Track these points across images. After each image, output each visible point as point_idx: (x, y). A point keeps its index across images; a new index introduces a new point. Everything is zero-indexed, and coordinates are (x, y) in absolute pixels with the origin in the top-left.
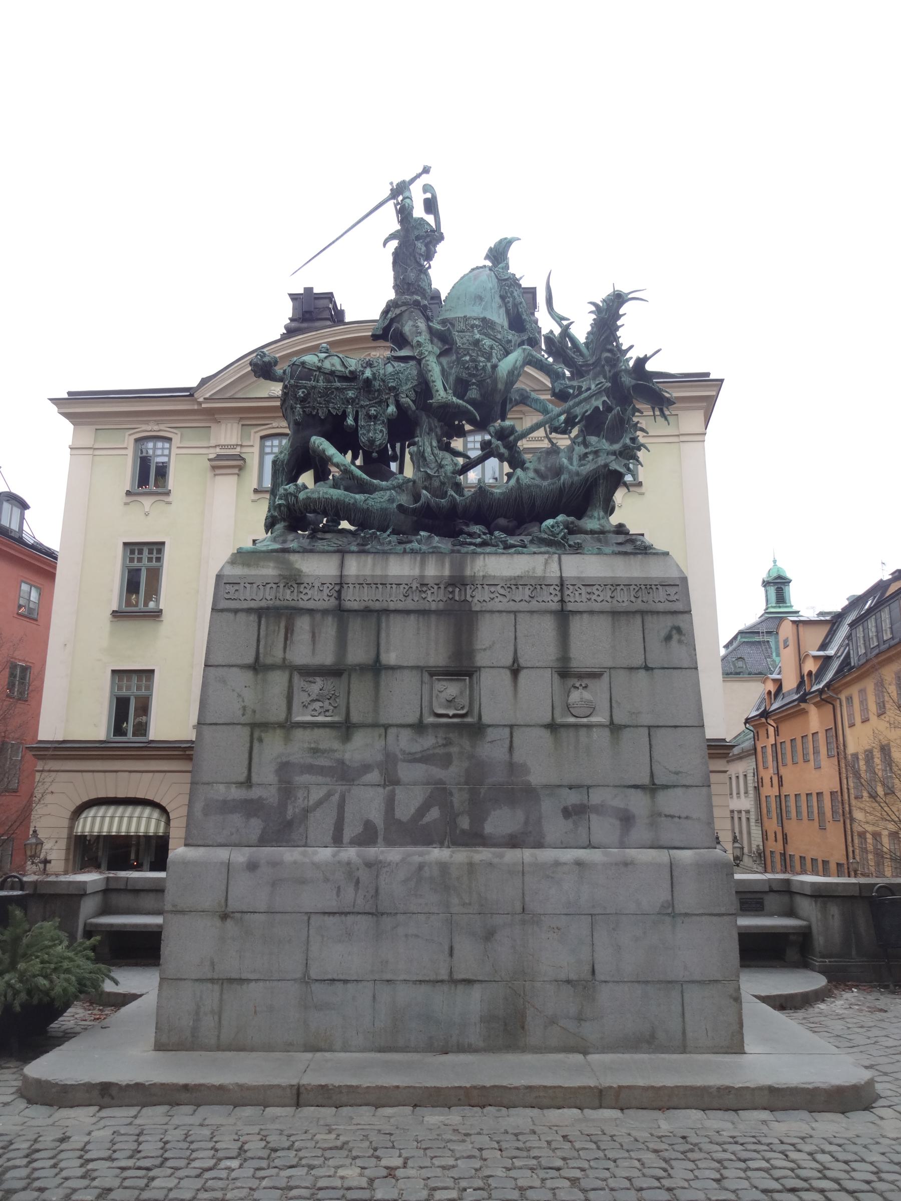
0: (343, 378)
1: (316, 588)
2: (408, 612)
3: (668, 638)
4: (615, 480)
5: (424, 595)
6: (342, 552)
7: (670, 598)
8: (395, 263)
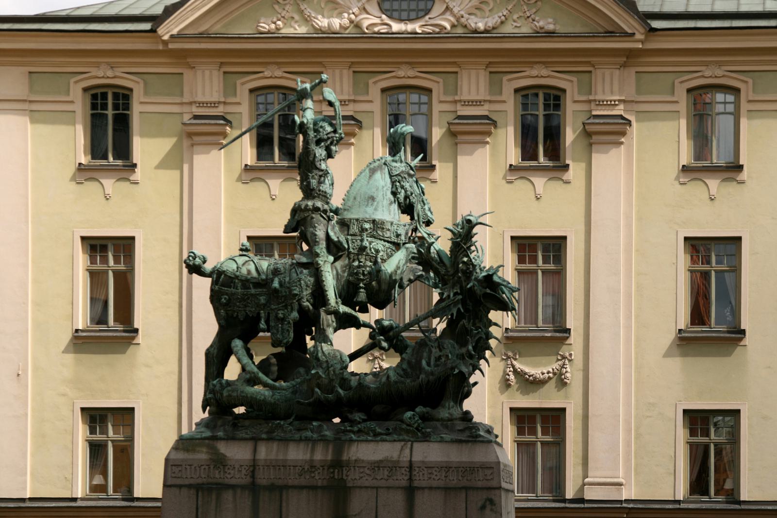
1: (237, 469)
2: (302, 488)
3: (483, 508)
5: (313, 475)
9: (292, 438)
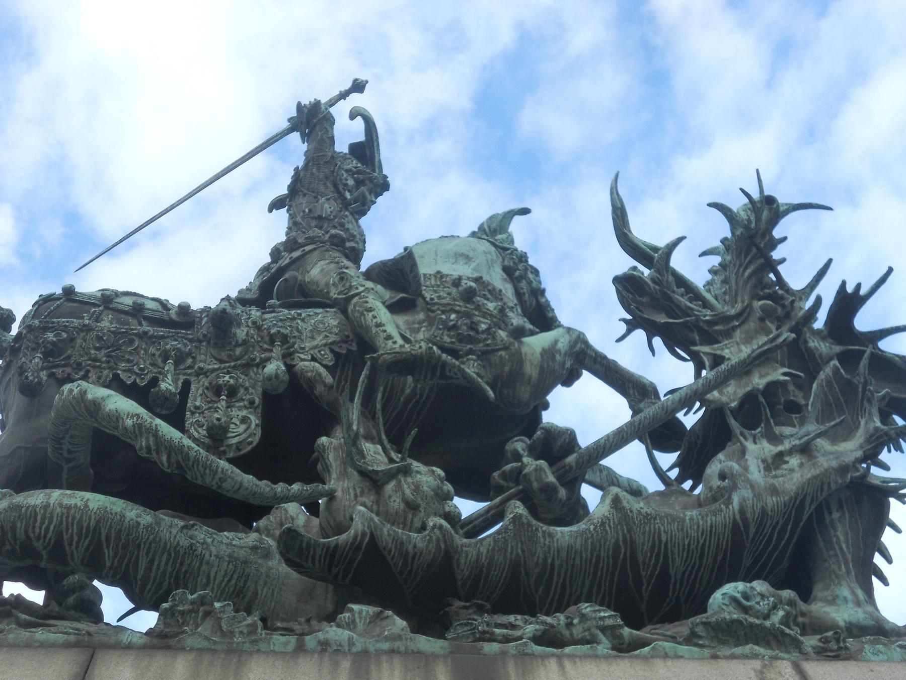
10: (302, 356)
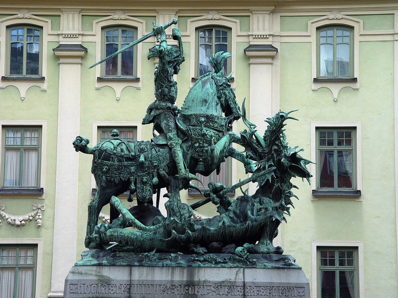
0: (128, 159)
1: (118, 287)
4: (278, 223)
5: (173, 291)
6: (130, 266)
7: (299, 295)
8: (156, 81)
9: (157, 265)
10: (161, 169)
